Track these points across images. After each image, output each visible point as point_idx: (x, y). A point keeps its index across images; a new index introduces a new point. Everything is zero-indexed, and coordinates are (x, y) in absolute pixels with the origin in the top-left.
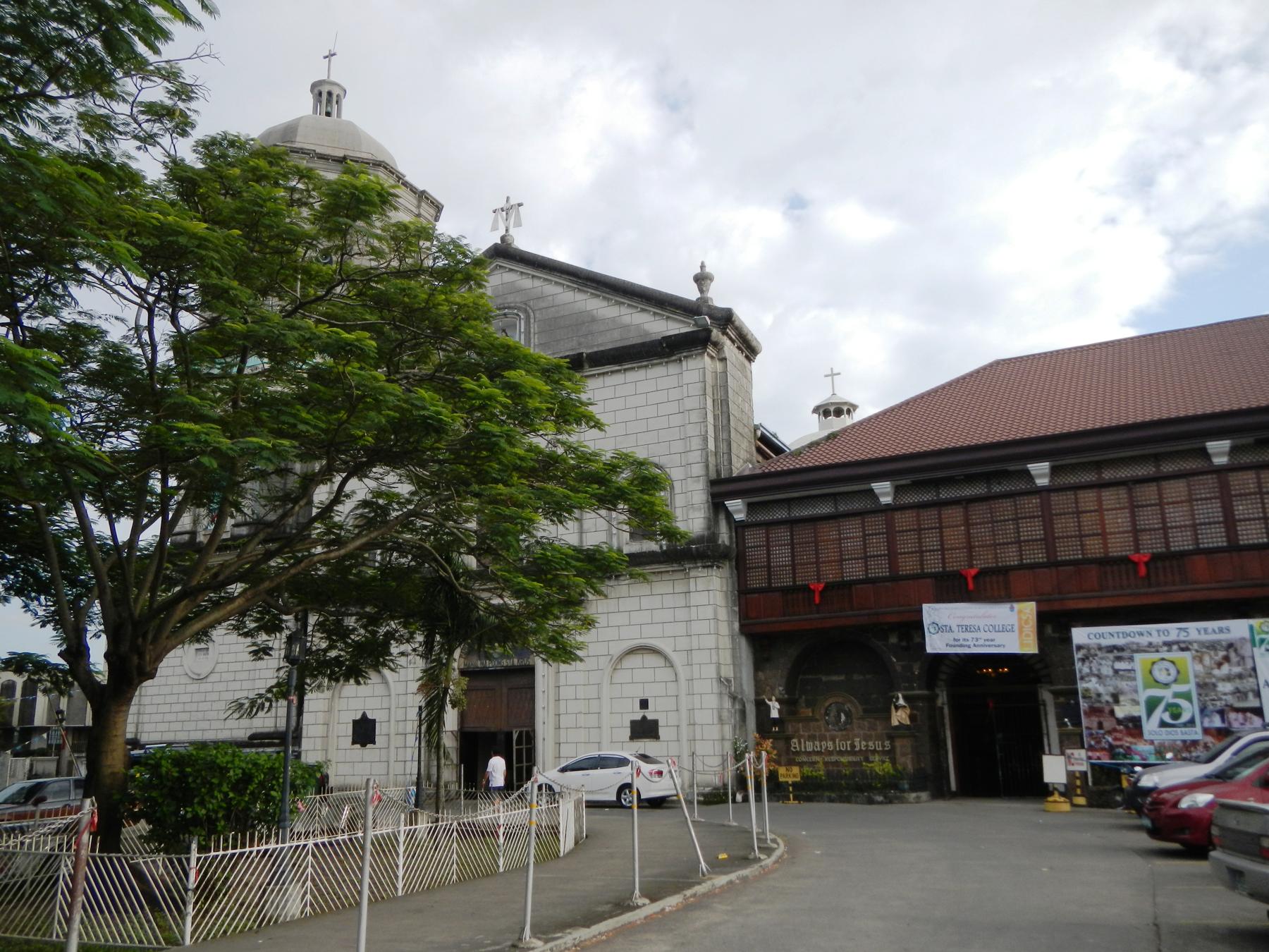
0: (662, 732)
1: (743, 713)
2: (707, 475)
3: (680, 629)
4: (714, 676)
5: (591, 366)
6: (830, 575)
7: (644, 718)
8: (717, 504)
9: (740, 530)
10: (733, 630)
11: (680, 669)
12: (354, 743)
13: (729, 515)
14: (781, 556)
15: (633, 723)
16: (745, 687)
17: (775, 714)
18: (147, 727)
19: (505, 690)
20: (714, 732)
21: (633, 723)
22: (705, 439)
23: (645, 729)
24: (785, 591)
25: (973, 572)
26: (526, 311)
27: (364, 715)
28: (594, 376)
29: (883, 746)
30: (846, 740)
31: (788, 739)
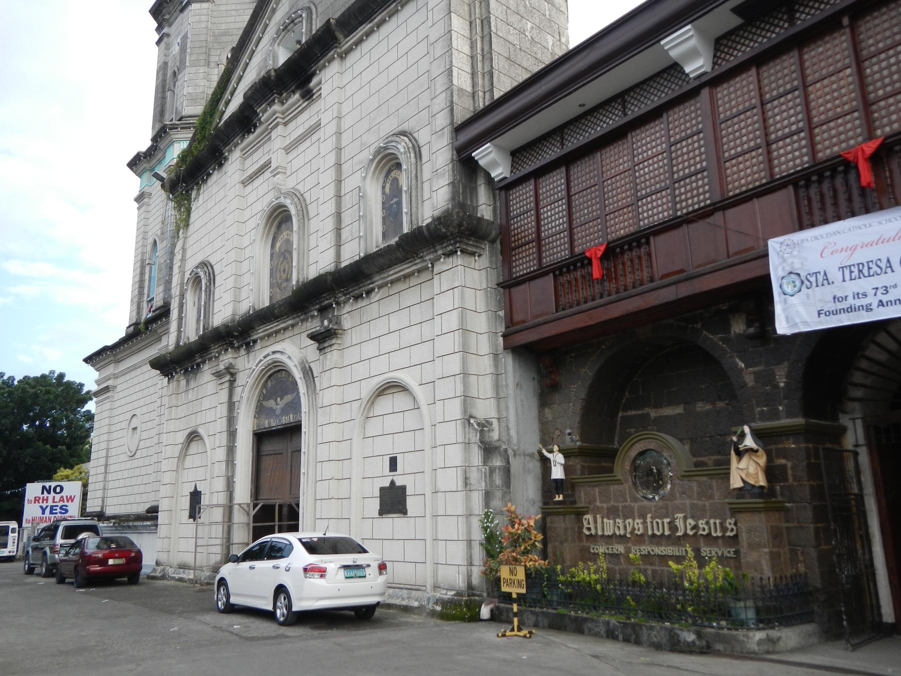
0: (410, 503)
1: (507, 471)
2: (452, 123)
3: (422, 353)
4: (459, 415)
5: (346, 37)
6: (621, 227)
7: (393, 482)
8: (466, 166)
9: (503, 193)
10: (496, 346)
11: (424, 409)
12: (190, 517)
13: (488, 175)
14: (554, 218)
15: (382, 489)
16: (513, 433)
17: (557, 473)
18: (109, 502)
19: (289, 454)
20: (456, 503)
21: (382, 489)
22: (450, 72)
23: (393, 501)
24: (559, 270)
25: (870, 147)
26: (309, 9)
27: (196, 487)
28: (349, 50)
29: (724, 529)
30: (662, 517)
31: (579, 514)
